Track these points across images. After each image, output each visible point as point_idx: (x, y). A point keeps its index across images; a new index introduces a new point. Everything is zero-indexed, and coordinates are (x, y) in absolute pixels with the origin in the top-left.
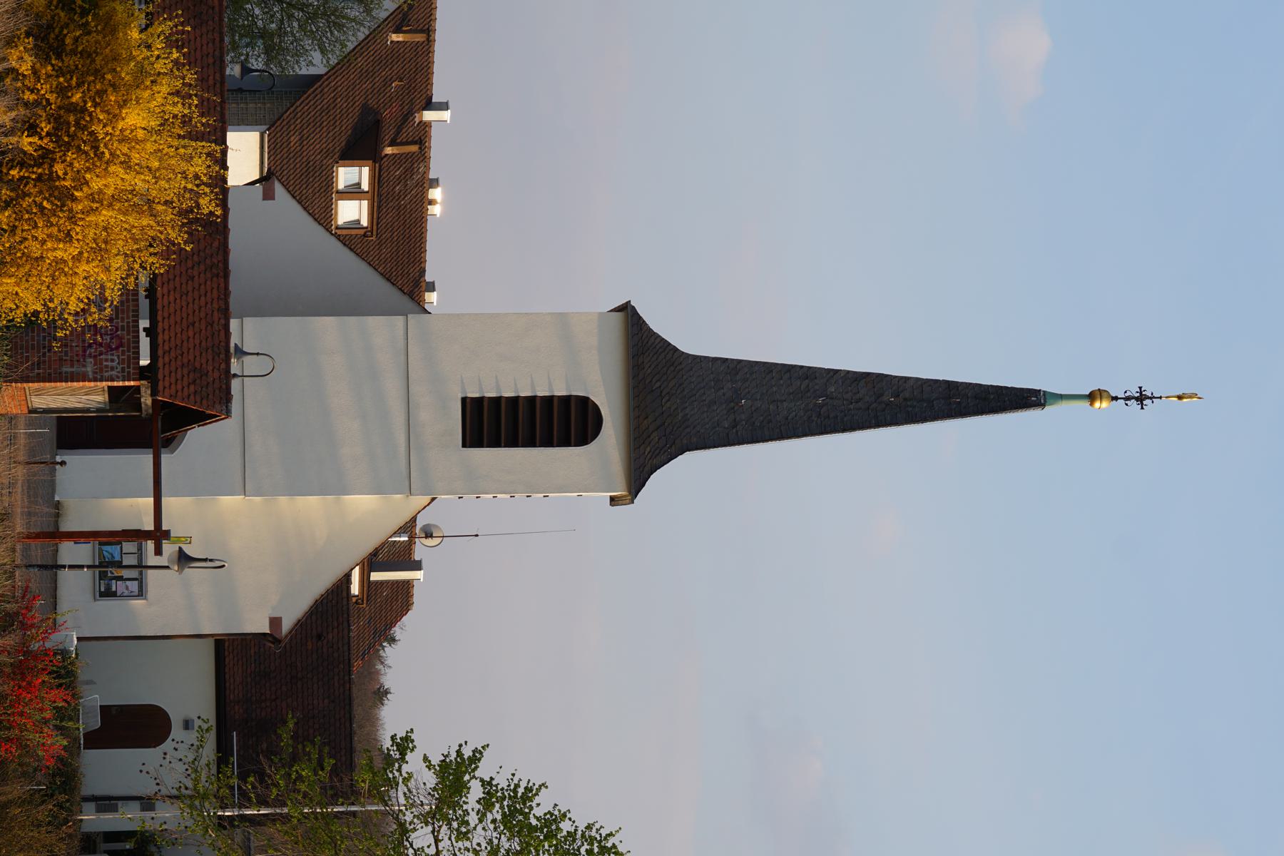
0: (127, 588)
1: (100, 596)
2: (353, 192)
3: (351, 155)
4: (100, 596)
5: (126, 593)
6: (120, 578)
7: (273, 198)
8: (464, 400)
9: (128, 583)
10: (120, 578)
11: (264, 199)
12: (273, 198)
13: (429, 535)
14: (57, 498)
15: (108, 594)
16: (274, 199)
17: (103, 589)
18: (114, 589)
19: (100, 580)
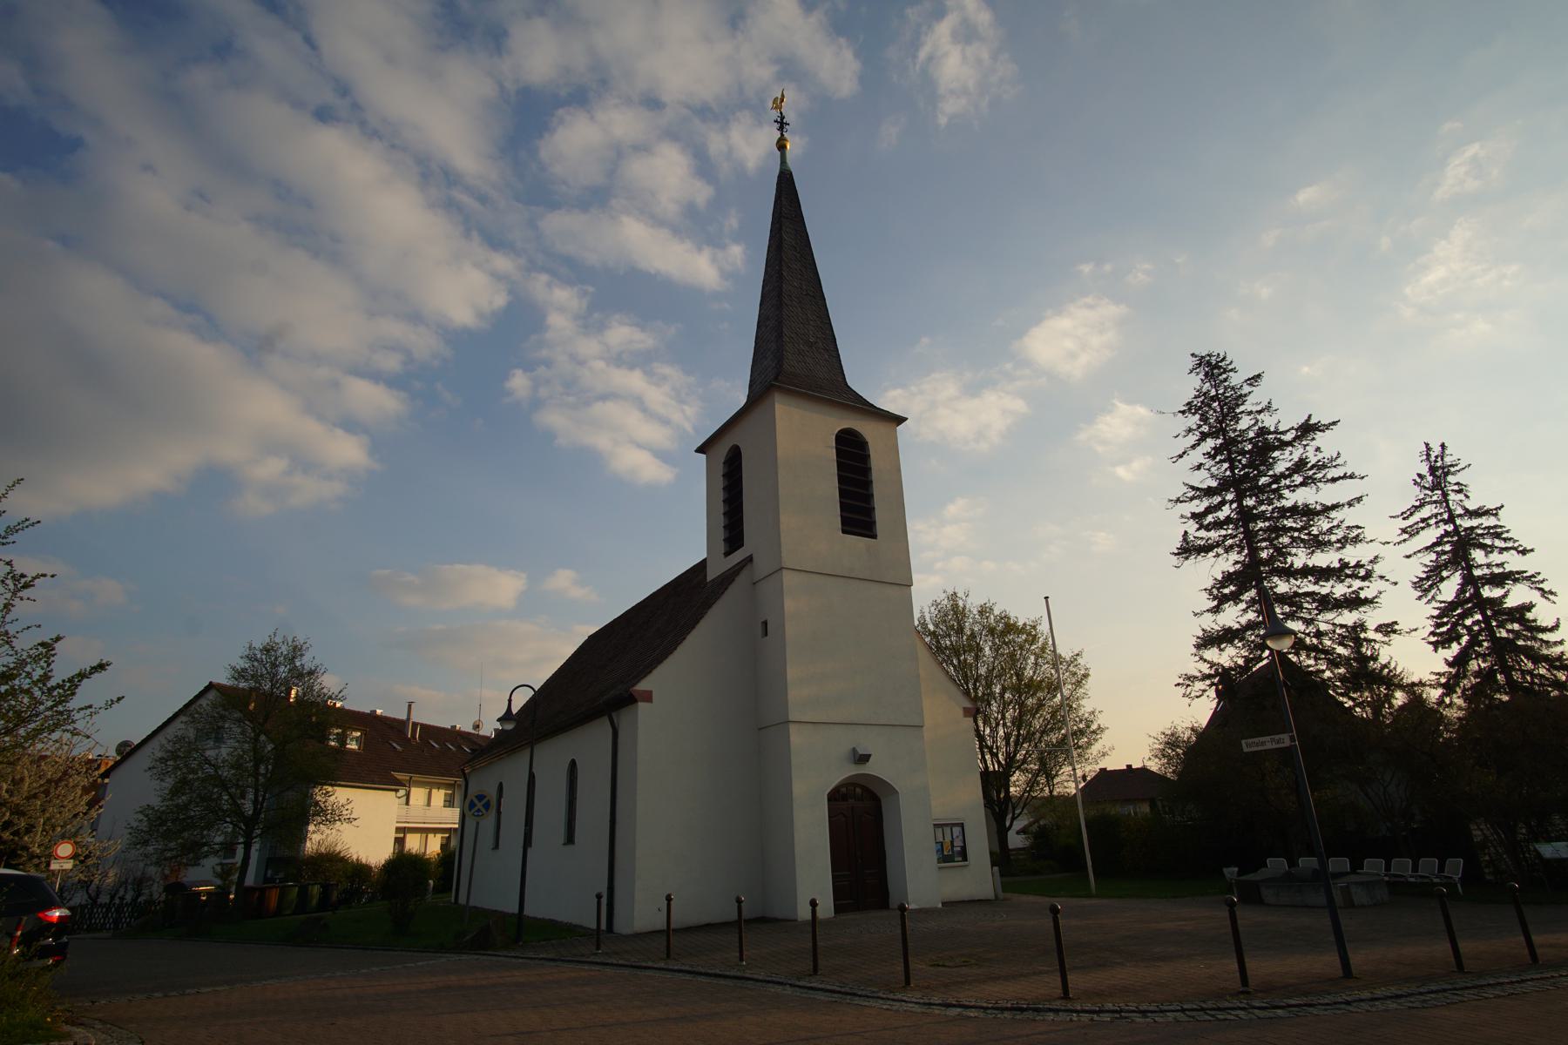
0: (957, 837)
1: (966, 860)
2: (342, 739)
3: (324, 738)
4: (966, 860)
5: (961, 837)
6: (952, 842)
7: (650, 693)
8: (844, 532)
9: (954, 837)
10: (952, 842)
11: (652, 702)
12: (650, 693)
13: (478, 726)
14: (940, 905)
15: (964, 854)
16: (651, 692)
17: (960, 859)
18: (959, 849)
19: (954, 861)
